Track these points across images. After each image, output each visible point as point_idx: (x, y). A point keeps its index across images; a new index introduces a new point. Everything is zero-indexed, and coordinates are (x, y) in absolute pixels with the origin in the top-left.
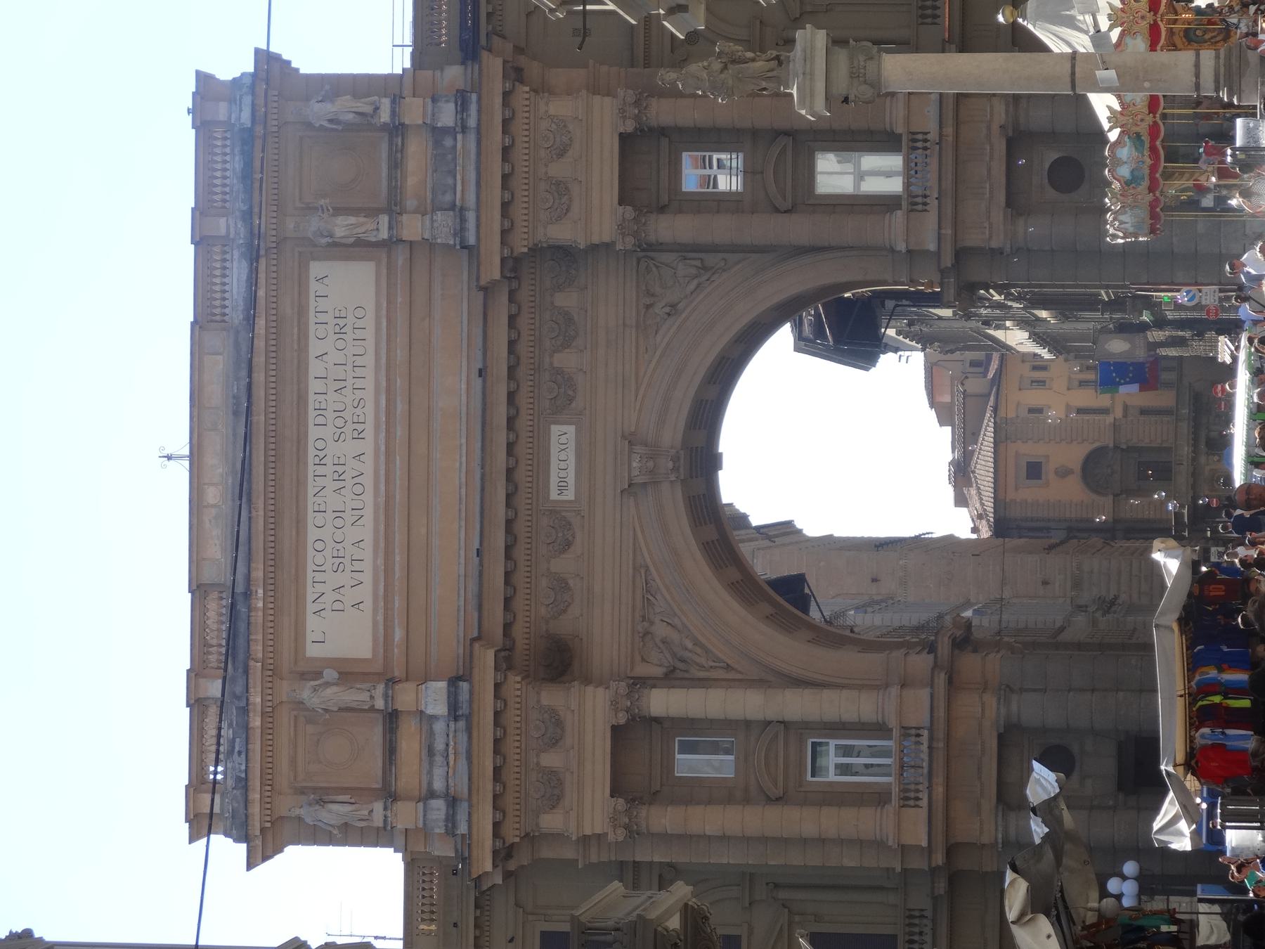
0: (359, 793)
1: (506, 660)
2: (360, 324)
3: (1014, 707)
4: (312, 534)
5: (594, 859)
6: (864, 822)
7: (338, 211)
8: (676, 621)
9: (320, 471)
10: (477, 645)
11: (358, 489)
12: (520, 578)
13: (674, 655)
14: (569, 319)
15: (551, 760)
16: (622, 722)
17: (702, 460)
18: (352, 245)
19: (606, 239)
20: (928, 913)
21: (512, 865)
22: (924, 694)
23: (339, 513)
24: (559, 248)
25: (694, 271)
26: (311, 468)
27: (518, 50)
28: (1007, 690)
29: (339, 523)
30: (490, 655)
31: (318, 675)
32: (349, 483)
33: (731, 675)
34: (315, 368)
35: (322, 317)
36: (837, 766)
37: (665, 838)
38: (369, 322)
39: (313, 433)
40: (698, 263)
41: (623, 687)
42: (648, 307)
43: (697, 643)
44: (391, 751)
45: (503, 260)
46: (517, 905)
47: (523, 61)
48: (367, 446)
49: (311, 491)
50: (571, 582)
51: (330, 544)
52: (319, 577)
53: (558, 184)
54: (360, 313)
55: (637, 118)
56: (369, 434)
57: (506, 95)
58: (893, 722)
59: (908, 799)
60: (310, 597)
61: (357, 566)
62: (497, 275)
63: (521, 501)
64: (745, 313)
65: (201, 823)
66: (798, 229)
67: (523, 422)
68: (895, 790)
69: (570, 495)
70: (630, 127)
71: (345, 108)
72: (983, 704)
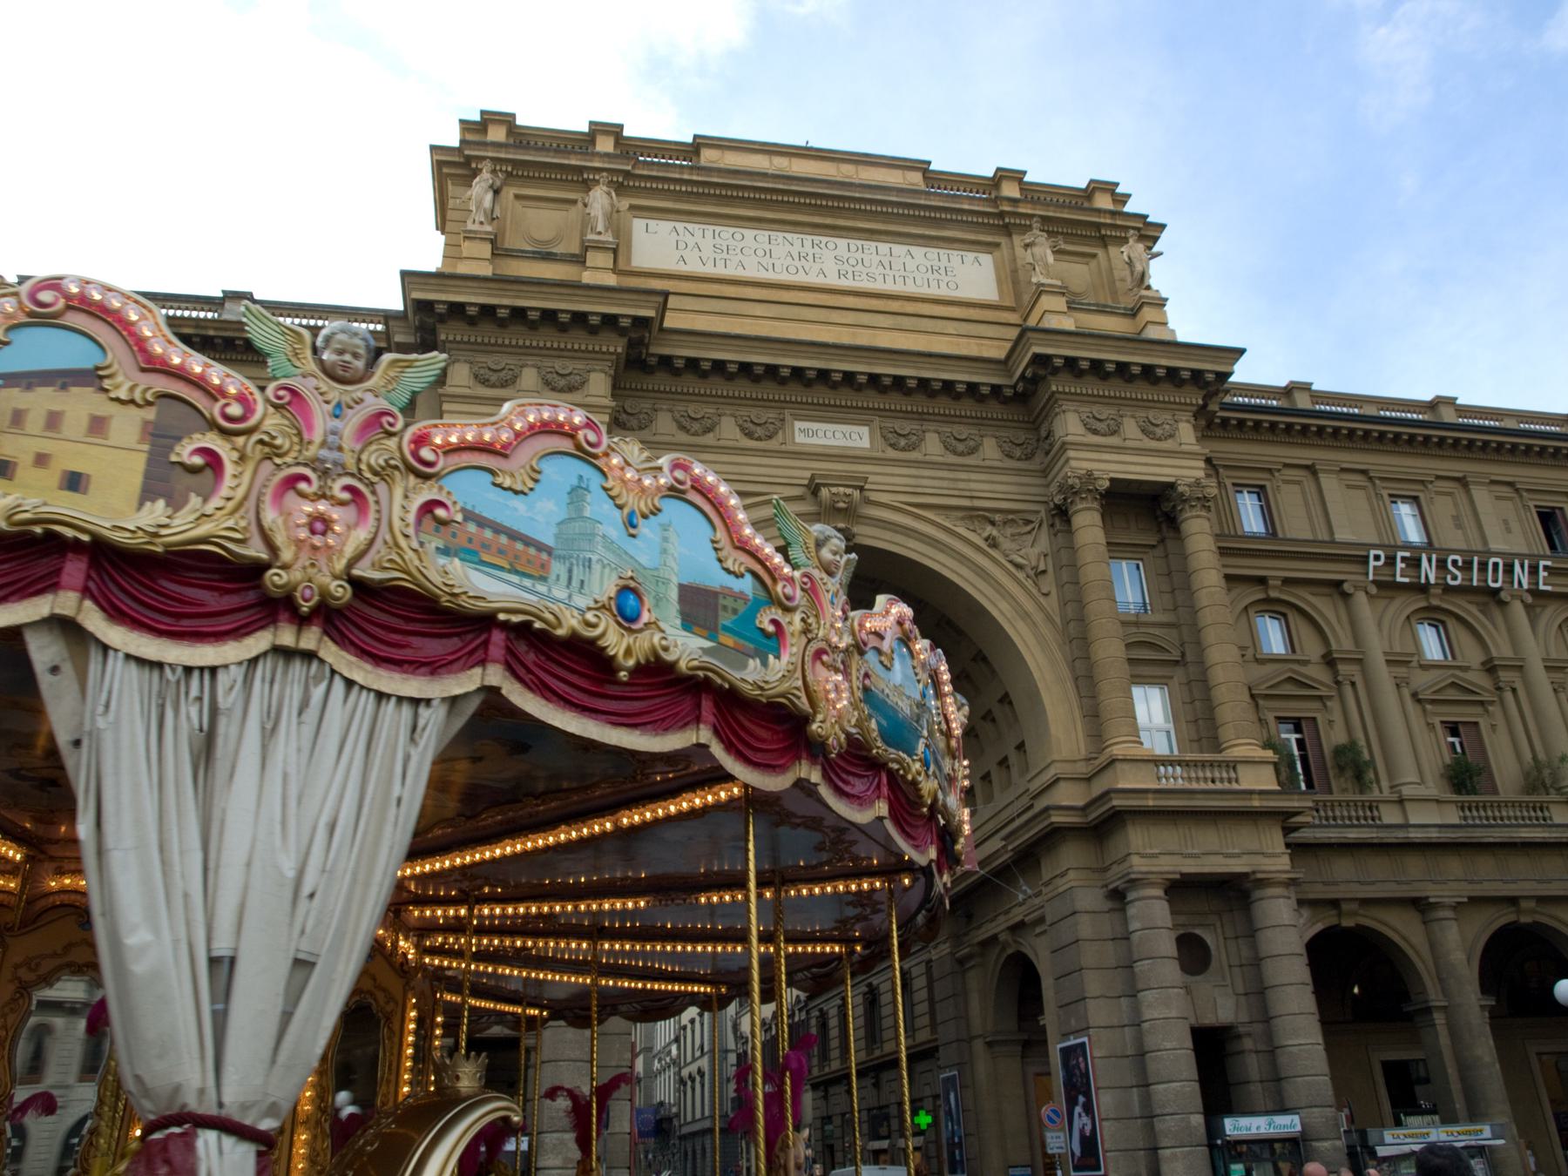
2: (943, 285)
4: (749, 234)
9: (808, 243)
12: (718, 386)
14: (972, 451)
15: (529, 377)
19: (1073, 463)
26: (810, 238)
30: (651, 313)
32: (798, 264)
34: (900, 250)
35: (944, 258)
38: (944, 292)
39: (842, 243)
48: (832, 281)
52: (709, 234)
53: (1119, 425)
60: (690, 226)
61: (720, 264)
63: (794, 392)
66: (1110, 651)
67: (876, 400)
69: (800, 438)
70: (1180, 489)
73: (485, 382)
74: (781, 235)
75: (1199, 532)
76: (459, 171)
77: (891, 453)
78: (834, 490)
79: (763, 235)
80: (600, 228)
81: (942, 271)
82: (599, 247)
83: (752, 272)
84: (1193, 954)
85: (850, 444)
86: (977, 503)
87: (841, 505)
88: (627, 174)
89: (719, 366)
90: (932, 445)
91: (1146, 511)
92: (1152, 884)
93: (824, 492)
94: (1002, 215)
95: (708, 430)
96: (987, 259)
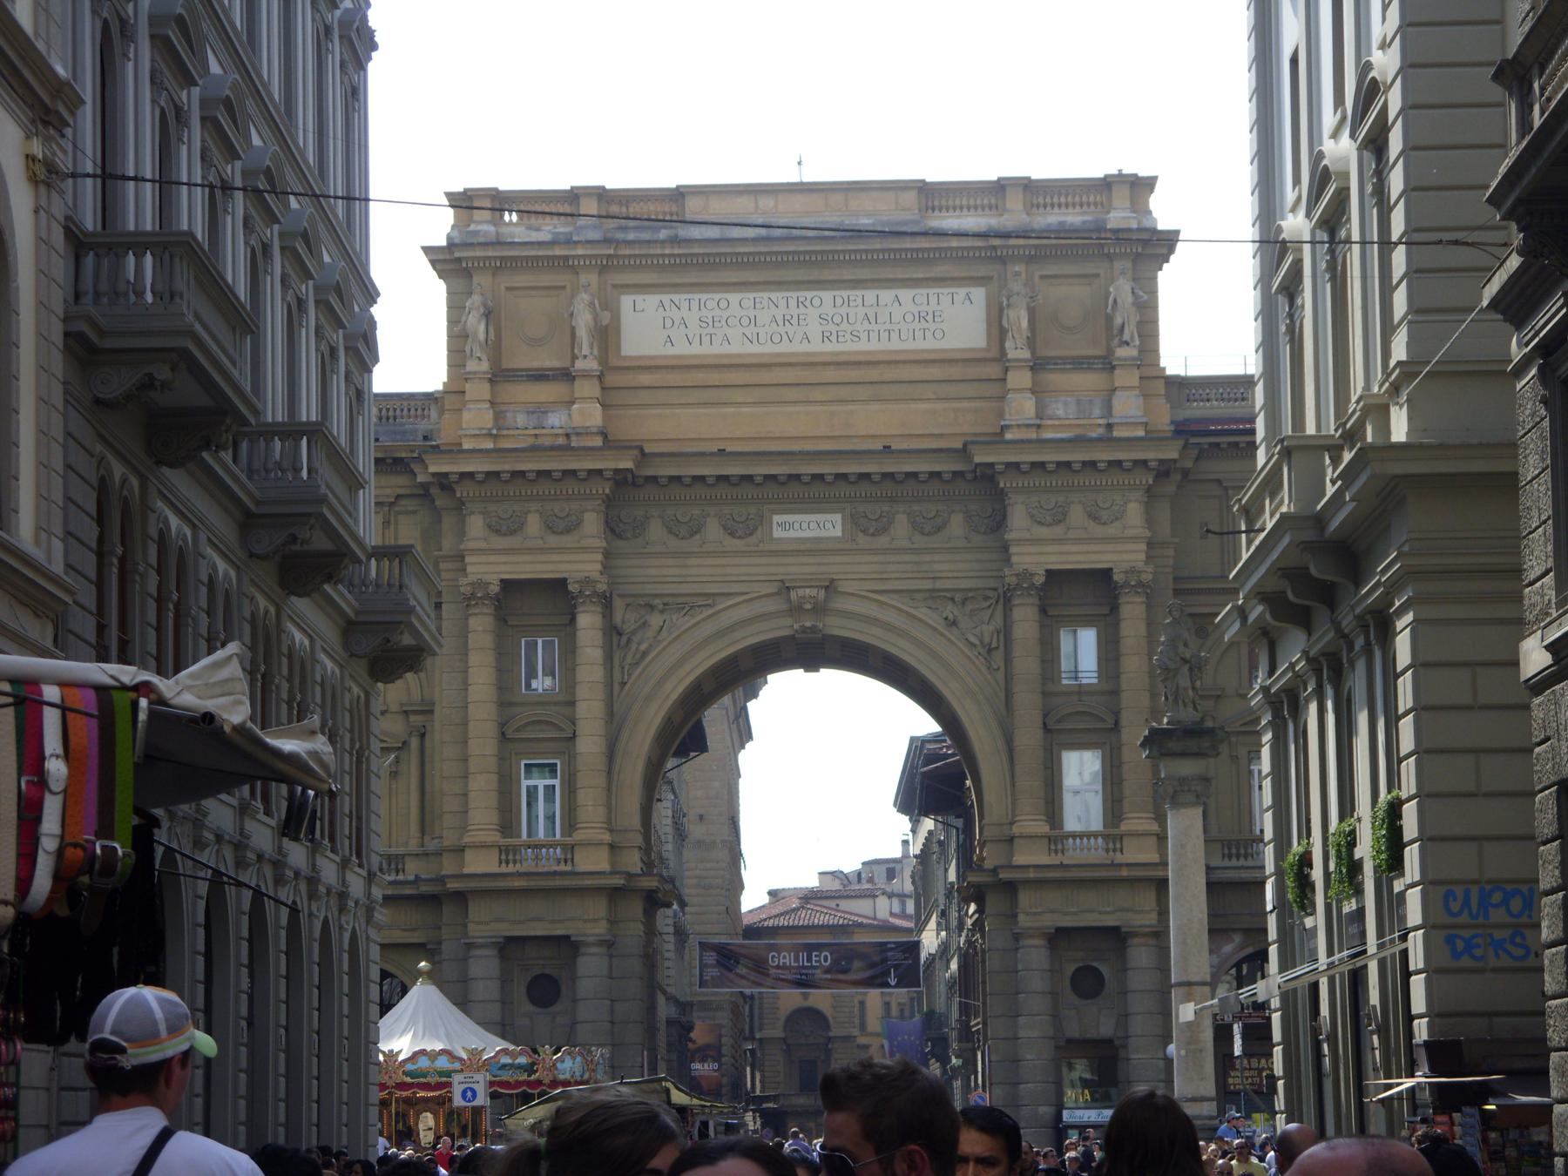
0: (495, 348)
1: (623, 481)
3: (594, 950)
4: (734, 298)
5: (442, 566)
6: (483, 817)
7: (1032, 313)
8: (664, 634)
9: (793, 303)
10: (636, 452)
11: (776, 339)
13: (633, 633)
14: (939, 529)
15: (534, 523)
16: (570, 588)
17: (812, 651)
18: (1001, 325)
19: (1014, 559)
20: (401, 877)
21: (434, 491)
22: (604, 866)
24: (1005, 517)
25: (987, 640)
26: (794, 294)
27: (1186, 473)
28: (609, 944)
29: (745, 321)
30: (629, 465)
31: (605, 307)
32: (782, 330)
33: (616, 688)
34: (886, 295)
35: (933, 299)
36: (536, 787)
37: (464, 632)
38: (930, 344)
39: (827, 296)
40: (994, 645)
41: (601, 587)
42: (952, 599)
43: (645, 654)
44: (539, 376)
45: (992, 465)
46: (398, 497)
47: (1178, 477)
48: (817, 346)
49: (774, 296)
50: (698, 537)
51: (725, 315)
52: (695, 305)
53: (1065, 514)
54: (939, 334)
55: (1126, 584)
56: (829, 347)
57: (1144, 463)
58: (578, 836)
59: (508, 853)
60: (676, 298)
61: (706, 340)
62: (977, 459)
64: (950, 691)
65: (463, 202)
66: (1029, 737)
68: (514, 841)
69: (778, 533)
70: (1116, 577)
71: (1125, 315)
72: (595, 921)
73: (498, 532)
74: (765, 295)
75: (1132, 612)
76: (452, 266)
77: (863, 541)
78: (801, 592)
79: (748, 297)
80: (585, 350)
81: (930, 318)
82: (586, 375)
84: (1088, 983)
85: (824, 534)
86: (939, 585)
87: (808, 606)
88: (609, 257)
90: (902, 527)
91: (1087, 593)
92: (1032, 936)
93: (793, 594)
94: (994, 248)
95: (693, 533)
96: (979, 294)
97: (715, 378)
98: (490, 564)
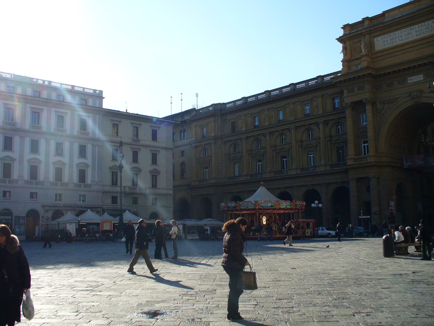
4: (396, 32)
9: (409, 30)
15: (356, 88)
23: (401, 36)
26: (409, 28)
29: (399, 37)
43: (384, 114)
48: (415, 38)
49: (405, 29)
52: (389, 36)
60: (385, 36)
69: (409, 82)
74: (403, 30)
83: (399, 43)
89: (389, 73)
93: (412, 95)
97: (393, 51)
98: (349, 99)
